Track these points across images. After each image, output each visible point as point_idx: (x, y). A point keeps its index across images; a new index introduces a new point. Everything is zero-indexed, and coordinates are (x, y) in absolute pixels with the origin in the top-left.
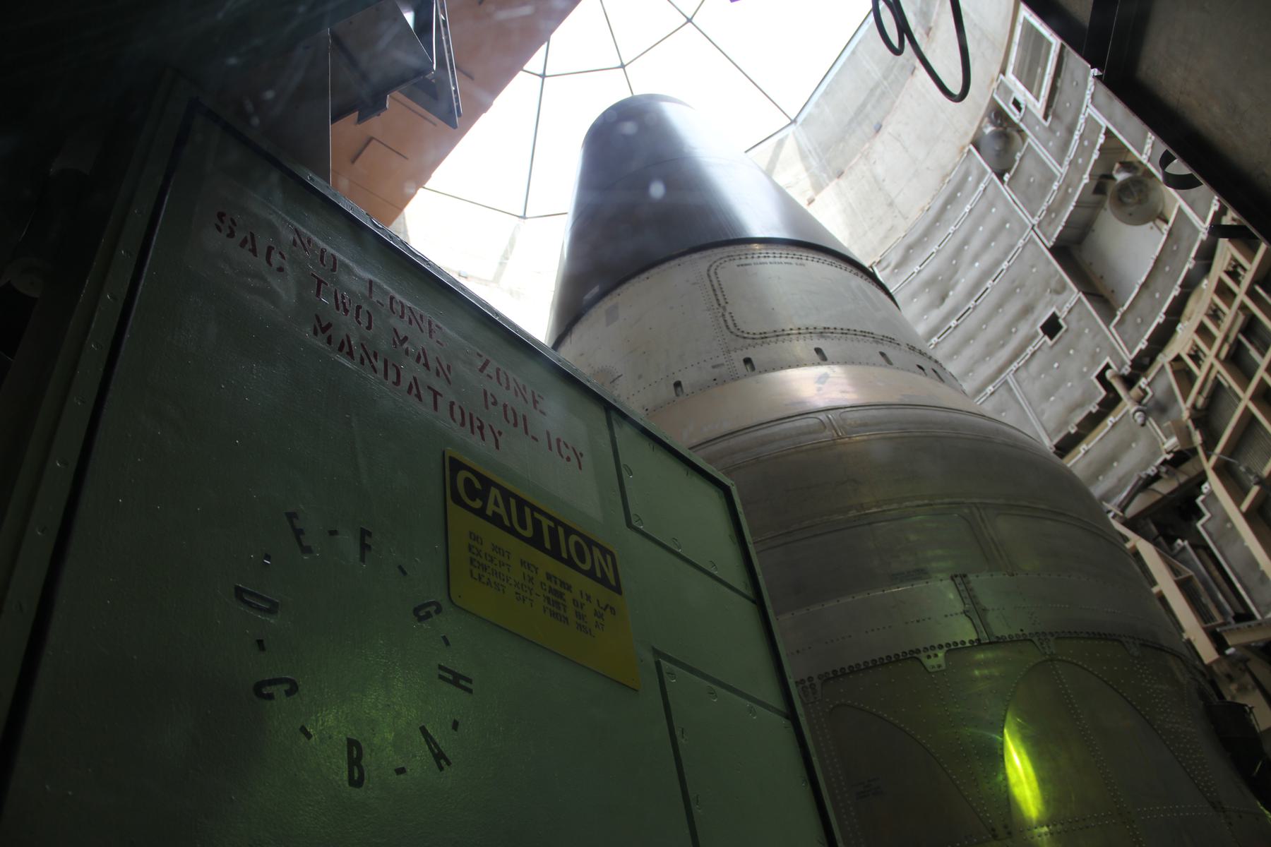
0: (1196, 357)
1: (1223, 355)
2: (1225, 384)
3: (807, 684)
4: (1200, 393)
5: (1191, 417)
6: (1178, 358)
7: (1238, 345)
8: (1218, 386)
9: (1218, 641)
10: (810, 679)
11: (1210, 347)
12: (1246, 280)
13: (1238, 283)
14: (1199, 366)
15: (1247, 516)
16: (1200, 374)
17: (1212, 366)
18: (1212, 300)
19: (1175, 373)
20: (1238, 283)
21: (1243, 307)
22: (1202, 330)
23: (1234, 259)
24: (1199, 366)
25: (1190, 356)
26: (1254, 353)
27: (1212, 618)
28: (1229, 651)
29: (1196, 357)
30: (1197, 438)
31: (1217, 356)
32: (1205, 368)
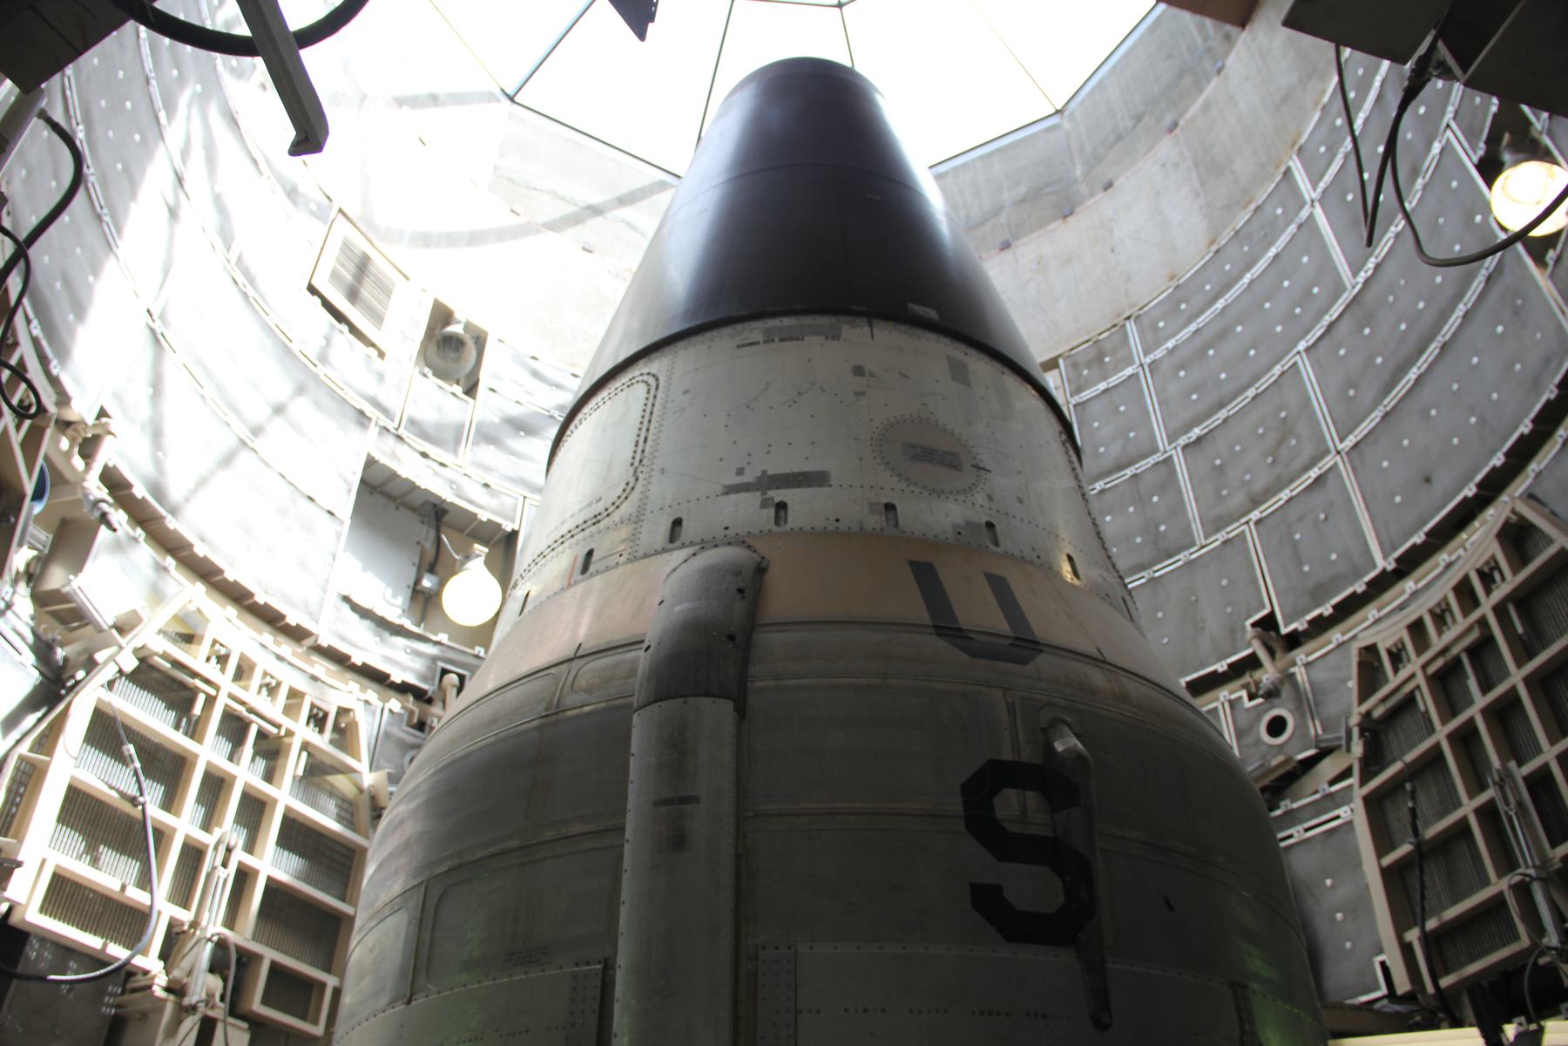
0: (1397, 657)
1: (1431, 670)
2: (1422, 708)
4: (1384, 700)
5: (1359, 725)
6: (1371, 649)
7: (1454, 667)
8: (1410, 701)
11: (1419, 652)
12: (1499, 593)
13: (1488, 591)
14: (1396, 670)
15: (1386, 873)
16: (1393, 681)
17: (1412, 676)
18: (1445, 599)
19: (1361, 664)
20: (1488, 591)
21: (1482, 622)
23: (1493, 558)
24: (1396, 670)
25: (1389, 652)
26: (1472, 684)
29: (1397, 657)
30: (1358, 748)
31: (1424, 667)
32: (1404, 673)
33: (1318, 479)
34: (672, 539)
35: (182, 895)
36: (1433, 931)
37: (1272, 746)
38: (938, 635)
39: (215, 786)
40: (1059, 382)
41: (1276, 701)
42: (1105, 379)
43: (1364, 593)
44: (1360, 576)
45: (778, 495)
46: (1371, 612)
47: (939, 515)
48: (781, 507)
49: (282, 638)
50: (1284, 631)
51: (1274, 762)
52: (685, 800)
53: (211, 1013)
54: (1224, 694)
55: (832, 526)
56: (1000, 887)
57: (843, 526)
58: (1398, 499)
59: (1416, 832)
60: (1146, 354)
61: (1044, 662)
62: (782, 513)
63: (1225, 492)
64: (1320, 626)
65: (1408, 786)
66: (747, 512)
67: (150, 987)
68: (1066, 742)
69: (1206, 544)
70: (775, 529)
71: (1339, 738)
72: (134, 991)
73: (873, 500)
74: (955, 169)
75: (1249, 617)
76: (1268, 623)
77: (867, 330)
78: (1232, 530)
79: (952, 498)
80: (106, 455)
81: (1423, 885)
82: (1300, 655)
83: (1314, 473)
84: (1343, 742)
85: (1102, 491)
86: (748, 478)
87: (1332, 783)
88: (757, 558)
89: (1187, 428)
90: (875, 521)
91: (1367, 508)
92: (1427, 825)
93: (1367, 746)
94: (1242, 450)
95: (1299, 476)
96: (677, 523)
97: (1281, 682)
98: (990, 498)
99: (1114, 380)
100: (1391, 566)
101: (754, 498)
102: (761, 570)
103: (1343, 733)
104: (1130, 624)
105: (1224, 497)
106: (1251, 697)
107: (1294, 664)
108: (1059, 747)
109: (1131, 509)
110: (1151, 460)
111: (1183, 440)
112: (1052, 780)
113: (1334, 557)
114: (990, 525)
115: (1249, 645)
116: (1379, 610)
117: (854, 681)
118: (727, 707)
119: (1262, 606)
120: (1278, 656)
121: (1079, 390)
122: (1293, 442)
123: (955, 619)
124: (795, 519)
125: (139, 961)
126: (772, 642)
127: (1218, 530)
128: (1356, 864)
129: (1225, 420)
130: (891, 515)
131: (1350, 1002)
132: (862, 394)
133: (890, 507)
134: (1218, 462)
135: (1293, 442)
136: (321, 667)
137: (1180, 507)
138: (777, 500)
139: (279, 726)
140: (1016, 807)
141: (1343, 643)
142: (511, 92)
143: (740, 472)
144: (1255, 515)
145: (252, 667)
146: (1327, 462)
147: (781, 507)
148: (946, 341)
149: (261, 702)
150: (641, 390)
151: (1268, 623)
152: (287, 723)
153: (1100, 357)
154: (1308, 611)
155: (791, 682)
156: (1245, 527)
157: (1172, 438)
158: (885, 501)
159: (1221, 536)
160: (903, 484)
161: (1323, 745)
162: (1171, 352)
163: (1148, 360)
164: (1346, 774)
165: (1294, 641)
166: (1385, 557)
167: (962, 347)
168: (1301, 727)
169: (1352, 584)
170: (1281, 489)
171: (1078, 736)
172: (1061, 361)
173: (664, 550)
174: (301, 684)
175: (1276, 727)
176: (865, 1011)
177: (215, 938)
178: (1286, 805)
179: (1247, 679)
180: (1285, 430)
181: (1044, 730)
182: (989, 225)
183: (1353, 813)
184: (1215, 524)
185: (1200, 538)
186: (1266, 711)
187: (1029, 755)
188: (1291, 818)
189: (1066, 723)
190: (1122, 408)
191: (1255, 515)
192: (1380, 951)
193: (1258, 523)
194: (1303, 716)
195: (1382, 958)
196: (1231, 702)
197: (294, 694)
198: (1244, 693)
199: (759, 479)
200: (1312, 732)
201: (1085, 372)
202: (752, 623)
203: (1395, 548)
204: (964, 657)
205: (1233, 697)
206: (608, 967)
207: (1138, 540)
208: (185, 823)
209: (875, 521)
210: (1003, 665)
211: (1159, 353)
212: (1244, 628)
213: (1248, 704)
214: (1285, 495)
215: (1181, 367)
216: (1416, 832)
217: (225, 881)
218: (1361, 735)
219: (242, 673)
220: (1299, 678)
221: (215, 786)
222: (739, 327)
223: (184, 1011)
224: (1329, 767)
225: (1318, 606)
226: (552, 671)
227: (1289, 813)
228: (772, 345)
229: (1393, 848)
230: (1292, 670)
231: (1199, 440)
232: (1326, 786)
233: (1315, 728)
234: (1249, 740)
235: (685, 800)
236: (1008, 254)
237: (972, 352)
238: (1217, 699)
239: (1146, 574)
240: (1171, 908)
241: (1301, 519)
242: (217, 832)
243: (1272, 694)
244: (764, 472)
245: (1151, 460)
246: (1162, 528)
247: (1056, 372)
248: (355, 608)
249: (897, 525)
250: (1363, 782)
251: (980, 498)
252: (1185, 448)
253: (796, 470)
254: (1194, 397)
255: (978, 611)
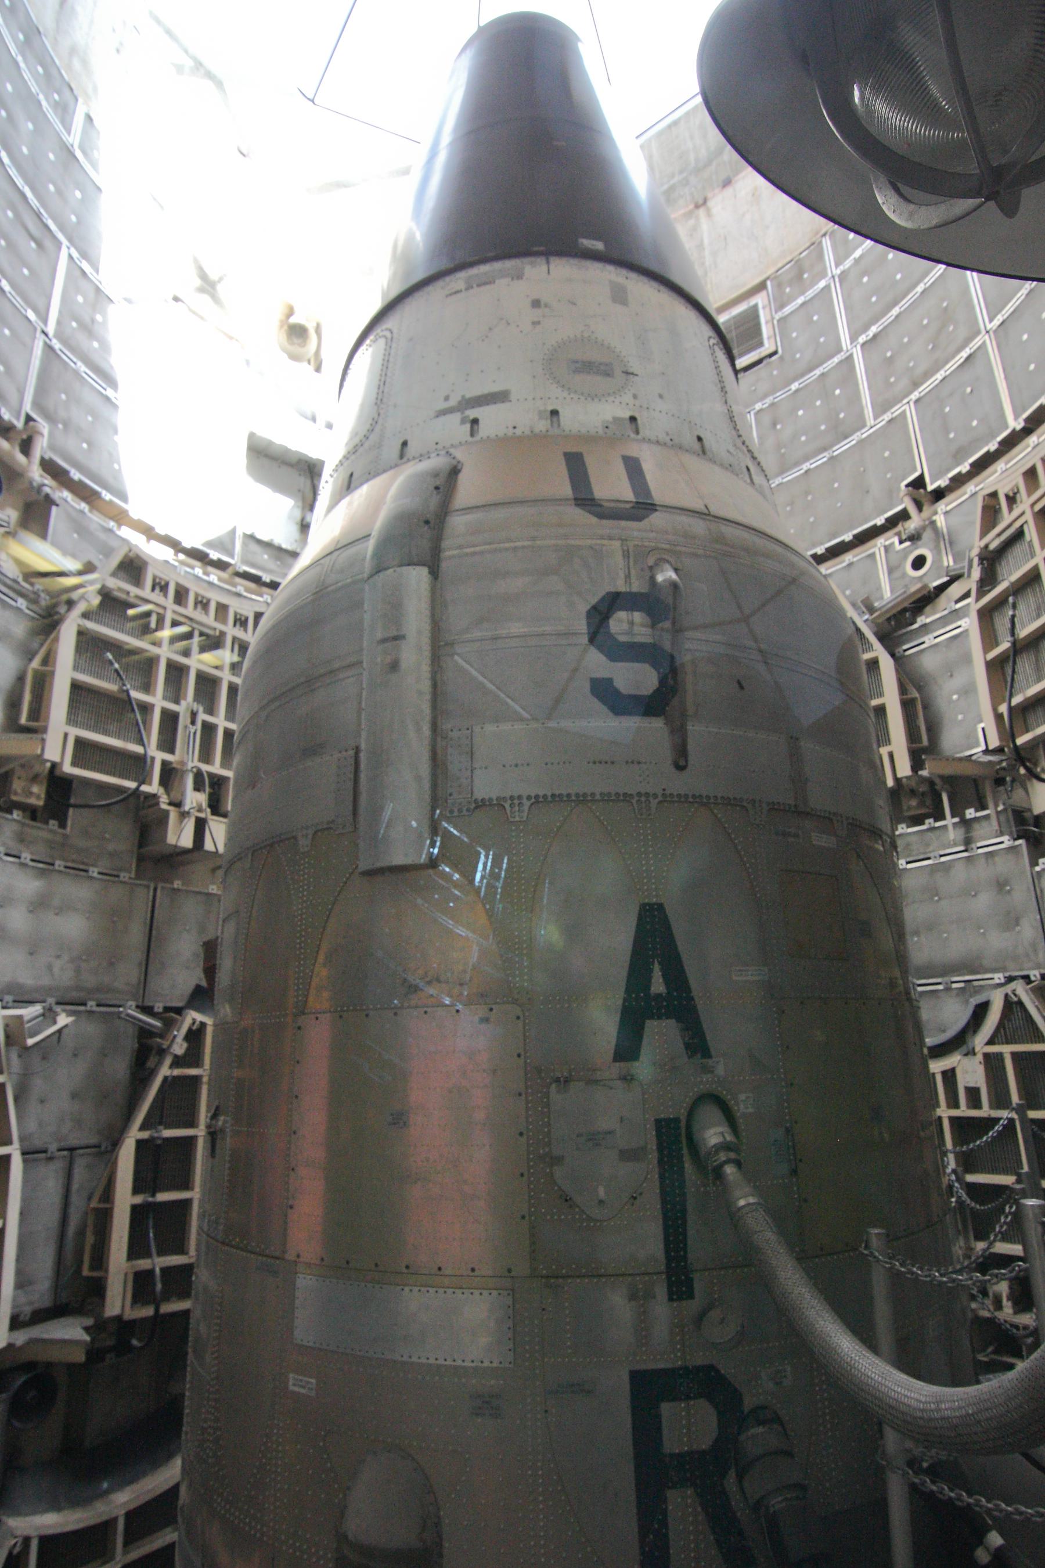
0: (1011, 500)
1: (1038, 507)
3: (516, 802)
4: (999, 535)
6: (994, 495)
8: (1019, 534)
9: (917, 764)
10: (520, 797)
15: (990, 665)
16: (1007, 517)
17: (1023, 513)
19: (985, 508)
22: (1031, 475)
25: (1007, 496)
27: (920, 741)
28: (924, 773)
30: (976, 573)
31: (1033, 505)
32: (1016, 512)
33: (968, 358)
34: (402, 456)
35: (168, 743)
36: (1018, 705)
37: (914, 578)
38: (577, 505)
39: (176, 672)
40: (766, 302)
41: (920, 543)
42: (803, 293)
43: (996, 451)
44: (994, 437)
45: (472, 413)
46: (1000, 466)
47: (587, 415)
48: (475, 422)
49: (210, 569)
50: (930, 488)
51: (913, 589)
52: (396, 638)
53: (202, 815)
54: (881, 541)
55: (510, 432)
56: (610, 681)
57: (518, 432)
58: (1032, 367)
59: (1013, 634)
60: (837, 266)
61: (656, 519)
62: (476, 427)
63: (892, 380)
64: (959, 481)
65: (1011, 599)
66: (454, 428)
67: (158, 804)
68: (666, 575)
69: (873, 423)
70: (470, 439)
71: (963, 567)
72: (150, 807)
73: (542, 408)
74: (687, 114)
75: (903, 480)
76: (919, 483)
77: (544, 267)
78: (896, 411)
79: (603, 400)
80: (41, 447)
81: (1014, 671)
82: (942, 506)
83: (964, 354)
84: (966, 570)
85: (797, 391)
86: (453, 402)
87: (957, 602)
88: (454, 462)
89: (866, 328)
90: (542, 426)
91: (1006, 378)
92: (1023, 627)
93: (984, 571)
94: (909, 341)
95: (953, 357)
96: (405, 444)
97: (924, 528)
98: (635, 397)
99: (810, 294)
100: (1019, 425)
101: (457, 417)
102: (454, 471)
103: (966, 563)
104: (750, 489)
105: (892, 384)
106: (901, 542)
107: (936, 513)
108: (660, 578)
109: (818, 403)
110: (836, 360)
111: (862, 339)
112: (653, 603)
113: (975, 423)
114: (633, 419)
115: (902, 502)
116: (1006, 464)
117: (512, 545)
118: (424, 571)
119: (915, 470)
120: (925, 508)
121: (782, 307)
122: (951, 328)
123: (592, 493)
124: (486, 430)
125: (144, 788)
126: (457, 523)
127: (884, 412)
128: (967, 659)
129: (897, 317)
130: (555, 419)
131: (958, 755)
132: (539, 323)
133: (554, 413)
134: (889, 354)
135: (951, 328)
136: (242, 586)
137: (855, 397)
138: (471, 418)
139: (215, 629)
140: (624, 624)
141: (976, 493)
142: (311, 97)
143: (447, 398)
144: (915, 396)
145: (187, 591)
146: (976, 343)
147: (475, 422)
148: (610, 268)
149: (198, 615)
150: (382, 342)
151: (919, 483)
152: (220, 626)
153: (799, 276)
154: (949, 470)
155: (468, 550)
156: (907, 408)
157: (853, 339)
158: (550, 408)
159: (887, 417)
160: (565, 394)
161: (951, 574)
162: (857, 261)
163: (838, 272)
164: (967, 595)
165: (939, 495)
166: (1016, 418)
167: (624, 272)
168: (938, 560)
169: (987, 444)
170: (938, 371)
171: (676, 570)
172: (769, 283)
173: (396, 466)
174: (225, 600)
175: (919, 562)
176: (516, 766)
177: (195, 770)
178: (921, 620)
179: (899, 528)
180: (946, 317)
181: (651, 568)
182: (714, 163)
183: (969, 623)
184: (880, 409)
185: (870, 420)
186: (911, 552)
187: (637, 586)
188: (925, 628)
189: (668, 562)
190: (815, 318)
191: (915, 396)
192: (981, 721)
193: (917, 402)
194: (939, 553)
195: (982, 725)
196: (885, 547)
197: (222, 608)
198: (896, 540)
199: (460, 402)
200: (946, 564)
201: (788, 290)
202: (444, 511)
203: (1024, 410)
204: (594, 520)
205: (887, 543)
206: (357, 750)
207: (823, 427)
208: (158, 700)
209: (542, 426)
210: (623, 523)
211: (848, 263)
212: (899, 488)
213: (898, 547)
214: (939, 376)
215: (865, 273)
216: (1013, 634)
217: (195, 733)
218: (981, 563)
219: (181, 596)
220: (939, 524)
221: (176, 672)
222: (447, 279)
223: (184, 815)
224: (956, 590)
225: (958, 465)
226: (322, 561)
227: (925, 625)
228: (471, 291)
229: (997, 645)
230: (934, 518)
231: (875, 336)
232: (953, 603)
233: (948, 561)
234: (897, 574)
235: (396, 638)
236: (729, 190)
237: (633, 276)
238: (876, 546)
239: (826, 455)
240: (742, 687)
241: (951, 395)
242: (183, 703)
243: (914, 538)
244: (463, 397)
245: (836, 360)
246: (842, 415)
247: (764, 294)
248: (259, 542)
249: (559, 425)
250: (977, 600)
251: (627, 398)
252: (863, 345)
253: (486, 392)
254: (874, 299)
255: (611, 485)
